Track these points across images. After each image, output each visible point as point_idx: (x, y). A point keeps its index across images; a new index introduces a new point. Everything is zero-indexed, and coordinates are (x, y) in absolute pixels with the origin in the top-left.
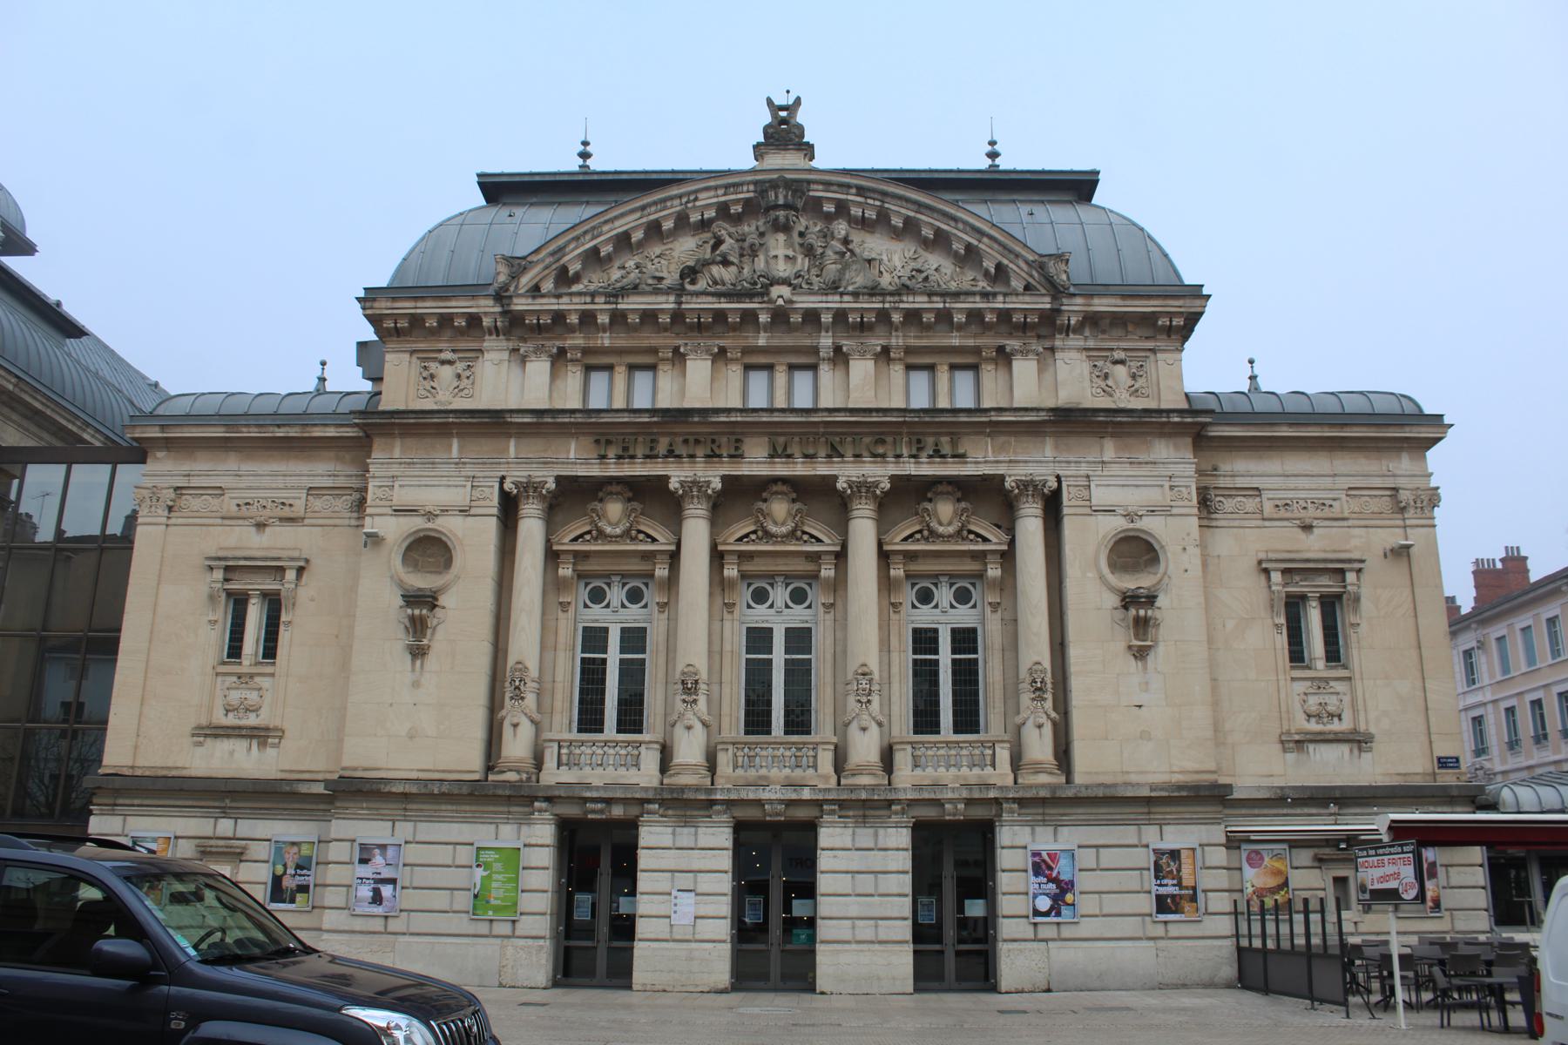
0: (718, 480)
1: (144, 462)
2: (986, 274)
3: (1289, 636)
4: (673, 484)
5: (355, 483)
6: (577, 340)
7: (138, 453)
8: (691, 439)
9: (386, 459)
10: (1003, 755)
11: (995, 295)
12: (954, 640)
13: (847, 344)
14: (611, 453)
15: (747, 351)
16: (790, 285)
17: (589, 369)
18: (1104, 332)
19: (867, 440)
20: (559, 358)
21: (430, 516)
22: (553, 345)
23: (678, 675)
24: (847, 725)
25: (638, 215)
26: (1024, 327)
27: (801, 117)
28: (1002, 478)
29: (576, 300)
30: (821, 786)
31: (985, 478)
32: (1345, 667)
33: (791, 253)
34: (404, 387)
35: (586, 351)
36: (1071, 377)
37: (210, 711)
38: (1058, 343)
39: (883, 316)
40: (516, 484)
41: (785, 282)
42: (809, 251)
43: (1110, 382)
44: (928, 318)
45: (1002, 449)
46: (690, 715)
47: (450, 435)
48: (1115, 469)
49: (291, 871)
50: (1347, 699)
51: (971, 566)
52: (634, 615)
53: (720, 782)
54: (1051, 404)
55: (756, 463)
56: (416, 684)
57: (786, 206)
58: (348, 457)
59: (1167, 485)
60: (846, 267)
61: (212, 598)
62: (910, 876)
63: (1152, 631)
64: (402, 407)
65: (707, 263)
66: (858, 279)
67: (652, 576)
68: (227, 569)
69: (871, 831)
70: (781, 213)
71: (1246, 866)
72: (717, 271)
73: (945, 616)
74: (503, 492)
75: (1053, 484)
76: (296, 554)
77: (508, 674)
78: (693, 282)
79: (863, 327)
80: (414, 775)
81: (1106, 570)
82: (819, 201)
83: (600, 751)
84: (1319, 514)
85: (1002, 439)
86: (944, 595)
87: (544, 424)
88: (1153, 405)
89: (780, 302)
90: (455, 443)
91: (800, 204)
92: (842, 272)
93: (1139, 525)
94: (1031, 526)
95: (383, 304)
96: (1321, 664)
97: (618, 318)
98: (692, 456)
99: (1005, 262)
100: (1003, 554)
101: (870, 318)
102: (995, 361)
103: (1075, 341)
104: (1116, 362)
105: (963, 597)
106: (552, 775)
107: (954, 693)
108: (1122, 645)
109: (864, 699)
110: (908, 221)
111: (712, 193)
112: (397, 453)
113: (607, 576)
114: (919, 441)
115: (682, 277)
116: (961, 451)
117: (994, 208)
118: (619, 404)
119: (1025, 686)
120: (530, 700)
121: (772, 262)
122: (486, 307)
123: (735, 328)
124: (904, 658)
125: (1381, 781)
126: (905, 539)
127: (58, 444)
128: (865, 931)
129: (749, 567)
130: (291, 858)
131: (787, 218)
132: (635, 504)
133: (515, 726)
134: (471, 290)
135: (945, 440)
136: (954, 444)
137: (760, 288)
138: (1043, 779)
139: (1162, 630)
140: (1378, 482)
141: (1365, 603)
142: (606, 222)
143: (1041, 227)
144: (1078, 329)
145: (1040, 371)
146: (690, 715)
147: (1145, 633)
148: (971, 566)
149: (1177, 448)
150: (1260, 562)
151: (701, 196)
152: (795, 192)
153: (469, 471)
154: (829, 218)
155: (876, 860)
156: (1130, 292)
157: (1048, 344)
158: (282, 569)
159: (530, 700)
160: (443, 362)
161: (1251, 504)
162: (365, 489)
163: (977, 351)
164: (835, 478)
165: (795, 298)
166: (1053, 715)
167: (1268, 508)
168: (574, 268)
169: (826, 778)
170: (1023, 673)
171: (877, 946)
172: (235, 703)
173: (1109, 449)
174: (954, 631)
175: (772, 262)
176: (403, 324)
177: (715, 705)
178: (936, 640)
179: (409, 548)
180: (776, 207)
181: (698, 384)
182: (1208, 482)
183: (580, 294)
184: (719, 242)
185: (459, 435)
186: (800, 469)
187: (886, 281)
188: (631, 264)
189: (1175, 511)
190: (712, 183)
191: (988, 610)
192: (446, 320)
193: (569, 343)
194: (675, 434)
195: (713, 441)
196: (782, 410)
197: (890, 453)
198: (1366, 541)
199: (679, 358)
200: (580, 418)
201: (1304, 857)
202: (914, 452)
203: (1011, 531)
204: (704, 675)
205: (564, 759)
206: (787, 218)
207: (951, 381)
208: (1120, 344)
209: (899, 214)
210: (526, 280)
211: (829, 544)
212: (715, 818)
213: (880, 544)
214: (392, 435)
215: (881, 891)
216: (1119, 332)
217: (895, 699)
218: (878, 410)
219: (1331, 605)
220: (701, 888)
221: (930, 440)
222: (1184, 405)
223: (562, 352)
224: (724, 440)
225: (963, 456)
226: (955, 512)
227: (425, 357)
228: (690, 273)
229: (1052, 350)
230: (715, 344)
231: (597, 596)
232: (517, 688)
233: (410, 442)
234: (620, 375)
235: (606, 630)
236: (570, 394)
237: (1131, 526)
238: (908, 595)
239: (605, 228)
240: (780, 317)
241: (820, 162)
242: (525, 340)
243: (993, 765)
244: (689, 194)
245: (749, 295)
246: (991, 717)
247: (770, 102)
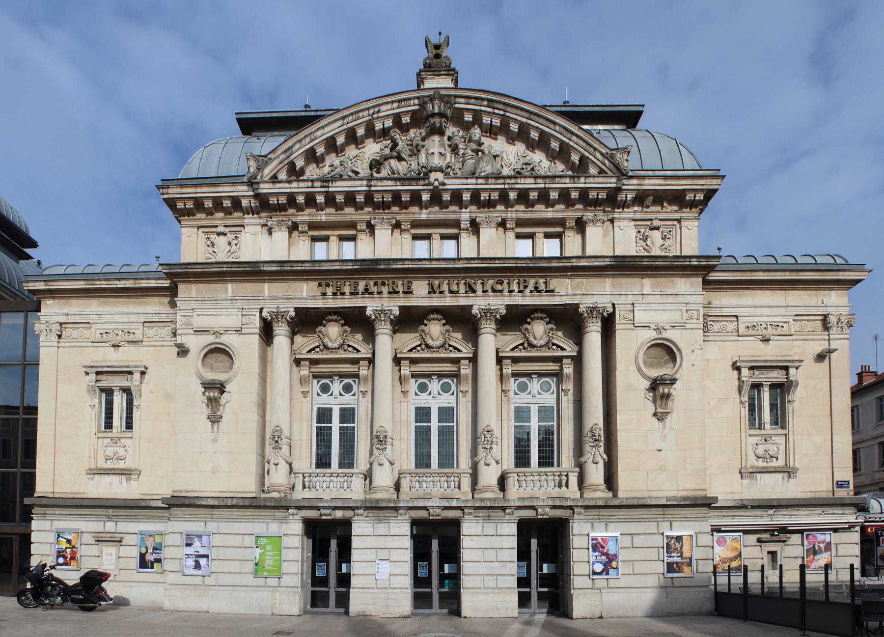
0: (397, 308)
4: (369, 312)
8: (380, 281)
10: (573, 480)
13: (481, 217)
14: (329, 291)
16: (442, 172)
19: (491, 282)
25: (340, 123)
28: (577, 306)
30: (462, 498)
33: (443, 152)
41: (441, 170)
42: (454, 149)
44: (534, 195)
45: (577, 286)
48: (650, 299)
49: (150, 551)
53: (402, 496)
55: (420, 295)
56: (215, 440)
57: (441, 115)
59: (684, 309)
60: (479, 160)
62: (516, 550)
64: (195, 261)
65: (387, 158)
69: (493, 525)
70: (437, 121)
71: (716, 545)
72: (393, 162)
79: (490, 204)
80: (217, 495)
81: (642, 365)
83: (328, 479)
87: (285, 272)
89: (436, 183)
91: (449, 113)
95: (175, 190)
97: (330, 200)
98: (380, 293)
99: (587, 154)
106: (300, 494)
110: (522, 125)
111: (389, 106)
115: (371, 169)
116: (551, 288)
120: (285, 449)
121: (430, 157)
122: (242, 190)
125: (800, 495)
128: (490, 582)
130: (150, 544)
131: (441, 124)
133: (276, 465)
134: (232, 180)
135: (542, 281)
137: (423, 175)
138: (599, 494)
142: (318, 129)
146: (382, 457)
149: (692, 284)
151: (382, 108)
152: (446, 103)
154: (467, 127)
155: (496, 542)
159: (285, 449)
164: (471, 306)
165: (446, 181)
166: (605, 456)
168: (300, 163)
169: (465, 493)
171: (496, 590)
173: (647, 284)
175: (430, 157)
180: (433, 115)
184: (395, 145)
186: (448, 301)
187: (505, 172)
188: (337, 162)
189: (688, 326)
190: (389, 99)
194: (370, 279)
195: (394, 283)
197: (506, 291)
201: (752, 539)
202: (522, 288)
205: (307, 484)
206: (441, 124)
210: (268, 171)
212: (400, 517)
215: (499, 560)
220: (394, 558)
224: (400, 282)
225: (553, 291)
228: (376, 165)
232: (276, 442)
237: (660, 336)
239: (319, 133)
243: (567, 486)
244: (374, 107)
245: (416, 180)
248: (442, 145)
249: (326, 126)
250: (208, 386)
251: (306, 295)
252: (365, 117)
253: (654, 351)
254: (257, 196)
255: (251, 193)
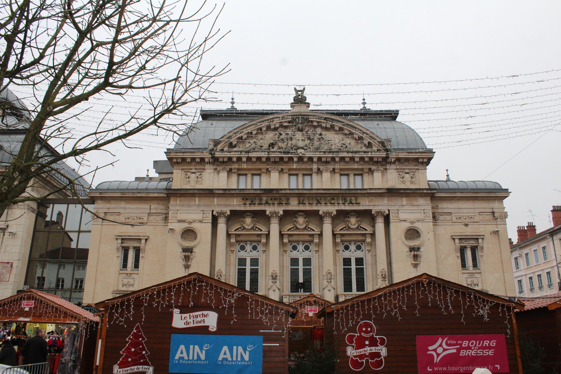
1: (94, 204)
2: (365, 145)
3: (461, 259)
4: (268, 213)
5: (164, 212)
6: (236, 166)
7: (92, 200)
8: (273, 198)
9: (175, 204)
11: (368, 152)
12: (356, 262)
13: (322, 168)
15: (290, 170)
17: (239, 175)
18: (402, 163)
19: (329, 198)
20: (230, 171)
21: (190, 223)
22: (228, 168)
23: (270, 274)
24: (324, 289)
25: (255, 126)
26: (377, 162)
27: (305, 94)
28: (371, 210)
29: (236, 153)
31: (366, 211)
32: (479, 269)
33: (303, 139)
34: (180, 180)
35: (238, 169)
36: (391, 178)
37: (118, 284)
38: (388, 167)
39: (333, 159)
40: (217, 213)
42: (309, 139)
43: (404, 179)
46: (274, 286)
47: (196, 197)
48: (406, 208)
50: (480, 280)
51: (361, 238)
52: (254, 254)
54: (386, 187)
55: (294, 205)
58: (161, 203)
59: (423, 212)
61: (117, 249)
63: (419, 259)
64: (180, 188)
66: (326, 148)
67: (260, 241)
68: (122, 239)
72: (280, 144)
73: (353, 254)
74: (213, 215)
75: (387, 212)
76: (145, 235)
77: (216, 273)
78: (273, 148)
79: (327, 162)
82: (312, 122)
84: (470, 220)
85: (371, 198)
86: (353, 247)
87: (226, 193)
88: (417, 187)
89: (301, 155)
90: (197, 199)
92: (320, 144)
93: (414, 225)
94: (380, 225)
95: (173, 154)
96: (471, 268)
97: (249, 159)
99: (371, 141)
100: (371, 234)
101: (329, 159)
102: (368, 173)
103: (393, 166)
104: (406, 173)
105: (359, 248)
107: (357, 279)
108: (410, 263)
109: (329, 281)
112: (178, 202)
113: (246, 242)
114: (345, 199)
115: (269, 146)
116: (358, 202)
117: (366, 122)
118: (249, 187)
119: (380, 276)
122: (207, 155)
123: (286, 162)
124: (341, 267)
126: (341, 230)
127: (62, 197)
129: (291, 239)
132: (255, 219)
135: (353, 198)
136: (356, 200)
139: (422, 259)
140: (488, 210)
141: (485, 249)
142: (244, 128)
143: (380, 130)
144: (394, 163)
145: (382, 176)
147: (417, 259)
148: (361, 238)
150: (452, 236)
151: (275, 120)
153: (202, 208)
154: (315, 127)
156: (409, 151)
157: (385, 167)
158: (140, 239)
160: (192, 173)
161: (448, 218)
162: (168, 214)
163: (362, 169)
164: (319, 211)
167: (454, 219)
170: (379, 272)
172: (126, 283)
173: (404, 201)
174: (356, 258)
175: (298, 142)
176: (179, 160)
177: (282, 284)
178: (350, 262)
179: (183, 233)
181: (274, 180)
182: (435, 211)
183: (237, 151)
184: (281, 134)
185: (198, 197)
186: (307, 208)
187: (333, 147)
189: (425, 221)
191: (367, 252)
192: (193, 159)
193: (233, 167)
196: (302, 189)
197: (336, 203)
198: (485, 229)
199: (268, 171)
200: (237, 192)
203: (374, 226)
204: (278, 274)
207: (354, 179)
208: (408, 167)
209: (337, 125)
210: (219, 147)
211: (317, 231)
213: (333, 231)
214: (177, 197)
216: (406, 164)
217: (338, 280)
218: (332, 189)
219: (474, 250)
221: (349, 198)
222: (428, 187)
223: (231, 169)
224: (283, 198)
225: (359, 203)
226: (356, 221)
227: (186, 171)
228: (272, 145)
229: (386, 169)
230: (280, 167)
231: (243, 248)
233: (182, 199)
234: (249, 177)
235: (246, 259)
236: (233, 183)
238: (341, 248)
240: (301, 159)
241: (312, 108)
242: (219, 166)
244: (271, 119)
246: (368, 286)
247: (295, 89)
248: (303, 135)
249: (248, 127)
250: (185, 250)
251: (236, 204)
252: (266, 123)
253: (409, 232)
254: (212, 158)
255: (210, 156)
